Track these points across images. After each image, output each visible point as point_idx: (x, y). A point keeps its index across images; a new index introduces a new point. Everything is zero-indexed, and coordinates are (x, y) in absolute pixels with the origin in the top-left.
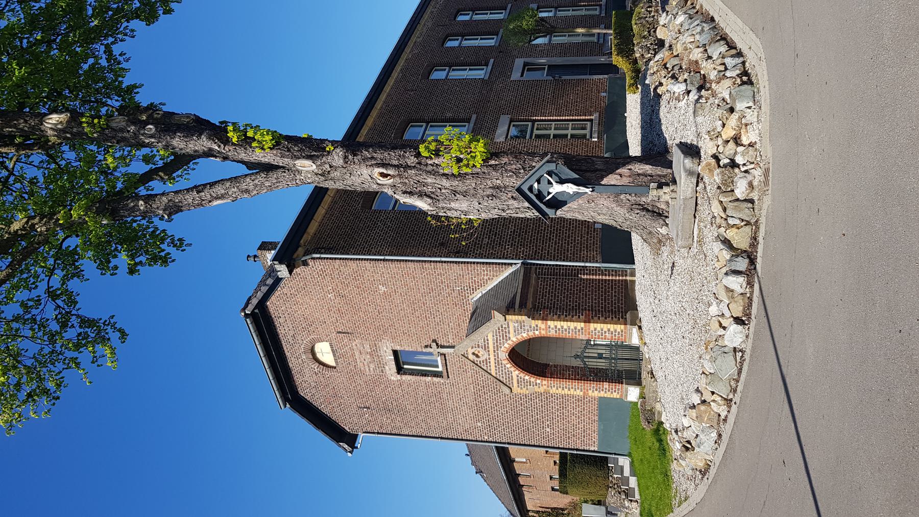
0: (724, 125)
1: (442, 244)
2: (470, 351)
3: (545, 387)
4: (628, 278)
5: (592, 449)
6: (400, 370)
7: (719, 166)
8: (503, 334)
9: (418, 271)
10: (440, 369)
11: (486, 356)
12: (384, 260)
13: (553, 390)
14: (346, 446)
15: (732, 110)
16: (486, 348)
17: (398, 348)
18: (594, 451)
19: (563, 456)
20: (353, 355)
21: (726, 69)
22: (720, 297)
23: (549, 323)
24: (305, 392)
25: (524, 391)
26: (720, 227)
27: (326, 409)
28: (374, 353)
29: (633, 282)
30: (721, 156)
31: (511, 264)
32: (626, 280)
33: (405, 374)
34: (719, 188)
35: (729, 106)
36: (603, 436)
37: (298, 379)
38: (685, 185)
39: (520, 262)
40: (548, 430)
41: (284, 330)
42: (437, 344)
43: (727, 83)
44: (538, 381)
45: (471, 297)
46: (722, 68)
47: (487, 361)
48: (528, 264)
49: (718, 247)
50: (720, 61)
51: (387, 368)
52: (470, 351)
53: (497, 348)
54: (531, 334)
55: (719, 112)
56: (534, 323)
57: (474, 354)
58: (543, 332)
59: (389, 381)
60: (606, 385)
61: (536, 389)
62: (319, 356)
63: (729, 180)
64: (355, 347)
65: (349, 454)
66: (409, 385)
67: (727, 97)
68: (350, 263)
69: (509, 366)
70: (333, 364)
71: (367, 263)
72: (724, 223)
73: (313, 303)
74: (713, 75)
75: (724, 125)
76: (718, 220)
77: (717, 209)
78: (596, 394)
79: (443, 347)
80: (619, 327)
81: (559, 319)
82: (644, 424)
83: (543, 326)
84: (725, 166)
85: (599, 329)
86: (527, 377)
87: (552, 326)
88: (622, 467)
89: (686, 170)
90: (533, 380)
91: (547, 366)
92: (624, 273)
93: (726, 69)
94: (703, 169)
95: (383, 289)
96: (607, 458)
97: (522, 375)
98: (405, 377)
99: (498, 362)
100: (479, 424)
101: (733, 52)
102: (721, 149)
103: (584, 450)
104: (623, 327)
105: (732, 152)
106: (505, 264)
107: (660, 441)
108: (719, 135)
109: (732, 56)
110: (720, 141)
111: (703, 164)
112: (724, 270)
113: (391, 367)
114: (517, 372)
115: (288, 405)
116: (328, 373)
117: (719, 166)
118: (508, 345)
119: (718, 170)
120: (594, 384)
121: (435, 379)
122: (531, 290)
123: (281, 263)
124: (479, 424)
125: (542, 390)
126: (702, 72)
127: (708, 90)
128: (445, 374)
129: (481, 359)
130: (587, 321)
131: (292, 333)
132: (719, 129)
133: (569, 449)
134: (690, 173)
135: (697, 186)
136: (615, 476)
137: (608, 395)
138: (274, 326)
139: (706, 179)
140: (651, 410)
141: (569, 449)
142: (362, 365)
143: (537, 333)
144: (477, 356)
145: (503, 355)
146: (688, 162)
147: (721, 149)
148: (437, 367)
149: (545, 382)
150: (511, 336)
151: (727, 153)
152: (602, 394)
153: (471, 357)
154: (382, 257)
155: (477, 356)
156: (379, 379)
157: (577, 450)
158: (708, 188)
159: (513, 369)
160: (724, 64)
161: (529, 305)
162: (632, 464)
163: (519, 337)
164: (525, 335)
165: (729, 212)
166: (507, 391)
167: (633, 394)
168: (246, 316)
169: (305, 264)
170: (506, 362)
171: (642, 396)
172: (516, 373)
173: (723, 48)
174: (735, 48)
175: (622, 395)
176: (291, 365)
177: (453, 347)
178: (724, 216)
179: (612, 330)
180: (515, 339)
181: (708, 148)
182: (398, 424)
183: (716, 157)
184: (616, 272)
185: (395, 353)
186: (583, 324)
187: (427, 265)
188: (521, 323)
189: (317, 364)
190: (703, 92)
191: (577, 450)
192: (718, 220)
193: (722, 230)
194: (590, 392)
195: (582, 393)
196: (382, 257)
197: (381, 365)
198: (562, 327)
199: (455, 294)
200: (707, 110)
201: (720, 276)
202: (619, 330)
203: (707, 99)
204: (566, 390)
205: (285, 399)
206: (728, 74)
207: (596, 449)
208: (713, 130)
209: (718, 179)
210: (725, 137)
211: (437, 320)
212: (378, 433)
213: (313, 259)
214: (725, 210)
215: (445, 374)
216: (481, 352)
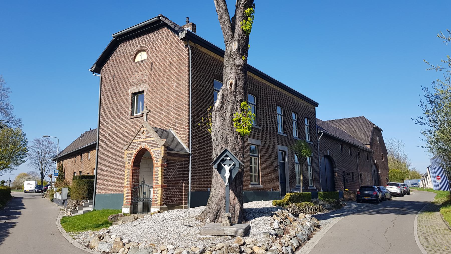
0: (260, 247)
1: (198, 114)
2: (145, 129)
3: (128, 167)
4: (184, 205)
5: (97, 191)
6: (134, 94)
7: (240, 246)
8: (155, 145)
10: (135, 114)
11: (143, 137)
12: (189, 85)
13: (126, 171)
14: (94, 68)
15: (267, 250)
16: (147, 137)
17: (145, 93)
18: (95, 192)
19: (93, 177)
20: (141, 71)
21: (286, 247)
22: (176, 250)
23: (160, 168)
24: (122, 47)
25: (125, 156)
26: (211, 248)
27: (113, 57)
28: (142, 81)
29: (182, 208)
30: (245, 246)
31: (189, 148)
32: (182, 204)
33: (132, 97)
34: (230, 246)
35: (269, 249)
36: (104, 197)
37: (128, 43)
38: (230, 230)
39: (190, 152)
40: (106, 169)
41: (152, 36)
42: (148, 113)
43: (279, 247)
44: (131, 163)
45: (172, 129)
46: (286, 245)
47: (140, 138)
48: (189, 156)
49: (201, 247)
50: (290, 243)
51: (135, 88)
52: (145, 129)
53: (147, 142)
54: (155, 159)
55: (265, 244)
56: (160, 160)
57: (144, 131)
58: (156, 165)
59: (128, 89)
60: (130, 197)
61: (127, 163)
62: (140, 54)
63: (233, 251)
64: (145, 72)
65: (90, 70)
66: (126, 99)
67: (273, 248)
68: (187, 68)
69: (138, 148)
70: (136, 61)
71: (187, 77)
72: (212, 249)
73: (166, 50)
74: (283, 241)
75: (260, 247)
76: (214, 247)
77: (219, 245)
78: (125, 192)
79: (147, 115)
80: (159, 202)
81: (162, 172)
82: (111, 216)
83: (159, 165)
84: (240, 248)
85: (158, 192)
86: (132, 158)
87: (159, 169)
88: (88, 207)
89: (237, 230)
90: (131, 160)
91: (139, 167)
92: (186, 203)
93: (286, 247)
94: (238, 238)
95: (175, 85)
96: (93, 199)
97: (134, 155)
98: (130, 98)
99: (140, 143)
100: (107, 135)
101: (294, 250)
102: (248, 246)
103: (96, 187)
104: (159, 204)
105: (247, 252)
106: (189, 145)
107: (103, 225)
108: (255, 245)
109: (292, 249)
110: (252, 245)
111: (241, 238)
112: (190, 251)
113: (135, 90)
114: (135, 153)
115: (114, 38)
116: (131, 58)
117: (240, 246)
118: (148, 147)
119: (238, 245)
120: (130, 191)
121: (130, 112)
122: (177, 158)
123: (186, 34)
124: (107, 135)
125: (127, 165)
126: (284, 236)
127: (276, 239)
128: (133, 117)
129: (141, 134)
130: (162, 186)
131: (151, 40)
132: (258, 245)
133: (96, 180)
134: (236, 232)
135: (230, 236)
136: (83, 203)
137: (125, 198)
138: (154, 31)
139: (233, 240)
140: (118, 219)
141: (96, 180)
142: (136, 75)
143: (155, 162)
144: (142, 133)
145: (143, 146)
146: (241, 231)
147: (248, 246)
148: (136, 113)
149: (130, 167)
150: (153, 149)
151: (246, 249)
152: (125, 195)
153: (142, 130)
154: (190, 84)
155: (142, 133)
156: (129, 84)
157: (96, 184)
158: (229, 241)
159: (136, 150)
160: (288, 246)
161: (169, 158)
162: (90, 211)
163: (153, 153)
164: (154, 156)
165: (218, 251)
166: (125, 148)
167: (126, 210)
168: (159, 17)
169: (186, 46)
170: (140, 147)
171: (125, 215)
172: (135, 152)
173: (295, 245)
174: (296, 251)
176: (135, 40)
177: (147, 120)
178: (216, 249)
179: (158, 198)
180: (152, 151)
181: (248, 240)
182: (106, 94)
183: (244, 244)
184: (186, 199)
185: (143, 92)
186: (160, 184)
187: (187, 107)
188: (160, 154)
189: (135, 53)
190: (275, 236)
191: (96, 184)
192: (214, 247)
193: (209, 249)
194: (126, 189)
195: (125, 185)
196: (190, 84)
197: (136, 85)
198: (158, 174)
199: (173, 121)
200: (267, 239)
201: (187, 249)
202: (158, 202)
203: (272, 238)
204: (127, 177)
205: (117, 37)
206: (284, 248)
207: (97, 193)
208: (257, 242)
209: (234, 245)
210: (254, 248)
211: (160, 112)
212: (101, 84)
213: (189, 50)
214: (219, 249)
215: (133, 117)
216: (145, 135)
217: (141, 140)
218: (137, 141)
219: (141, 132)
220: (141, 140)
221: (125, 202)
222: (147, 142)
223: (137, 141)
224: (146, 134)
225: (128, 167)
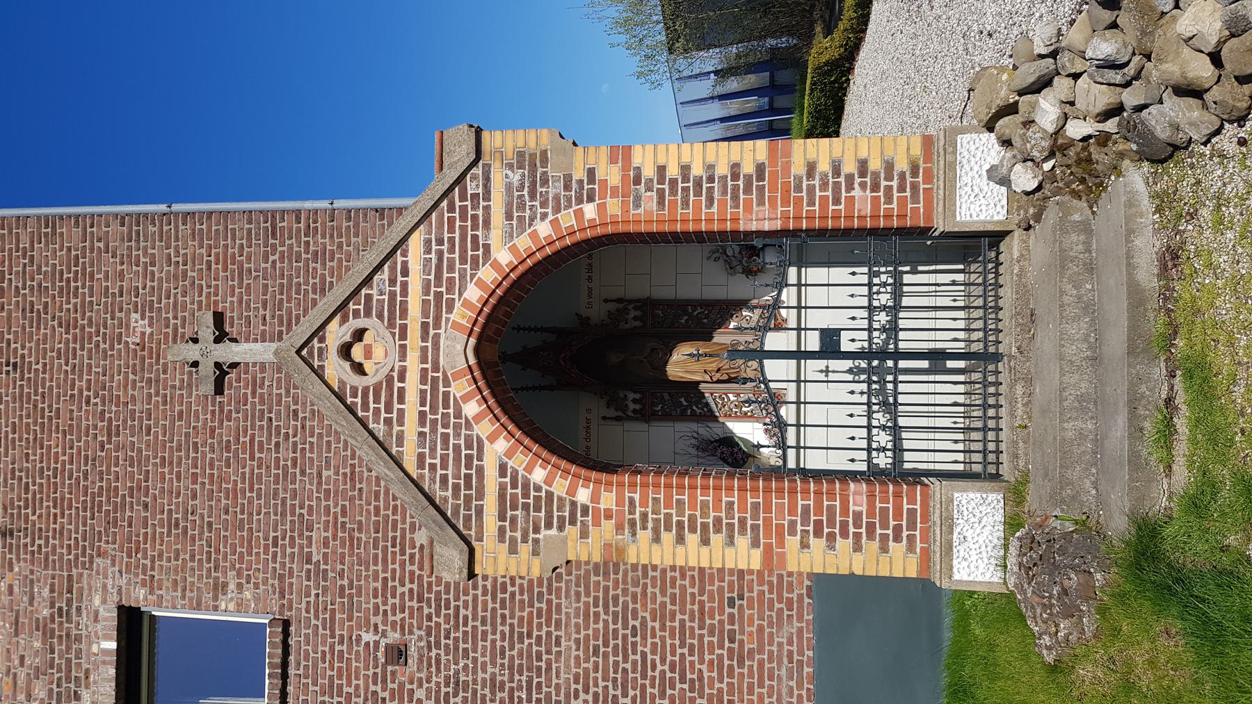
2: (337, 333)
3: (608, 526)
9: (257, 248)
13: (641, 550)
16: (395, 313)
17: (139, 597)
47: (390, 388)
53: (437, 307)
54: (567, 219)
57: (345, 351)
58: (614, 207)
69: (472, 409)
85: (824, 166)
86: (538, 475)
87: (649, 172)
90: (560, 487)
95: (139, 324)
97: (519, 462)
99: (432, 380)
114: (502, 445)
129: (369, 381)
143: (590, 211)
144: (359, 369)
145: (457, 350)
149: (608, 500)
150: (495, 237)
153: (335, 369)
155: (359, 369)
159: (484, 428)
163: (524, 243)
172: (500, 448)
175: (926, 556)
185: (131, 623)
194: (793, 542)
211: (286, 454)
217: (412, 385)
218: (411, 428)
219: (353, 379)
220: (412, 385)
221: (900, 563)
222: (437, 307)
223: (411, 428)
224: (372, 323)
225: (608, 526)
